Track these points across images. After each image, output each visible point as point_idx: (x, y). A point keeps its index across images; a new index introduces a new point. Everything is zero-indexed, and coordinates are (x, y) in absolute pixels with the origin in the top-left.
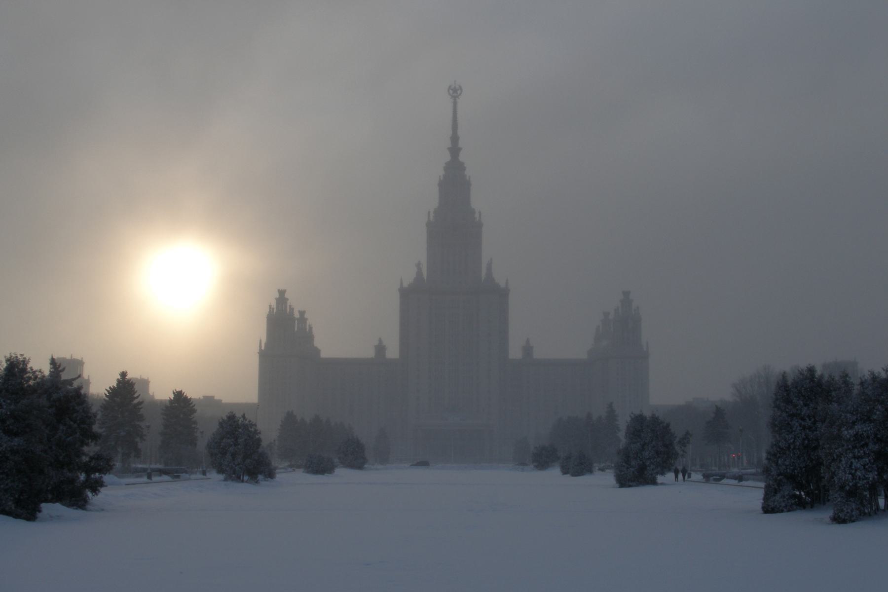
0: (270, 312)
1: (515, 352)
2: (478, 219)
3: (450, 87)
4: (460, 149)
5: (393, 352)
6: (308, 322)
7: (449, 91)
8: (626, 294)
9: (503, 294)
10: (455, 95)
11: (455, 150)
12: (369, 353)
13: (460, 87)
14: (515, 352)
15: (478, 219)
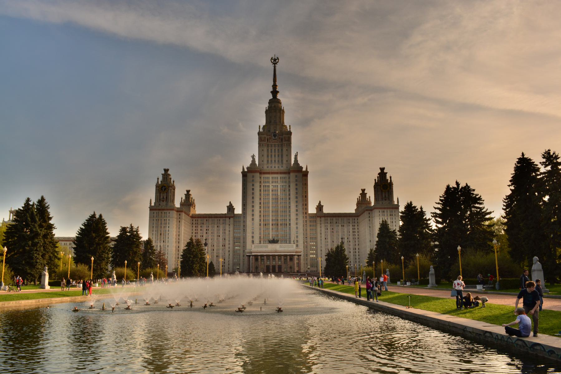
0: (158, 182)
1: (312, 210)
2: (289, 130)
3: (272, 58)
4: (278, 92)
5: (238, 210)
6: (191, 197)
7: (271, 60)
8: (382, 169)
9: (306, 174)
10: (275, 62)
11: (275, 92)
12: (225, 211)
13: (278, 58)
14: (312, 210)
15: (289, 130)
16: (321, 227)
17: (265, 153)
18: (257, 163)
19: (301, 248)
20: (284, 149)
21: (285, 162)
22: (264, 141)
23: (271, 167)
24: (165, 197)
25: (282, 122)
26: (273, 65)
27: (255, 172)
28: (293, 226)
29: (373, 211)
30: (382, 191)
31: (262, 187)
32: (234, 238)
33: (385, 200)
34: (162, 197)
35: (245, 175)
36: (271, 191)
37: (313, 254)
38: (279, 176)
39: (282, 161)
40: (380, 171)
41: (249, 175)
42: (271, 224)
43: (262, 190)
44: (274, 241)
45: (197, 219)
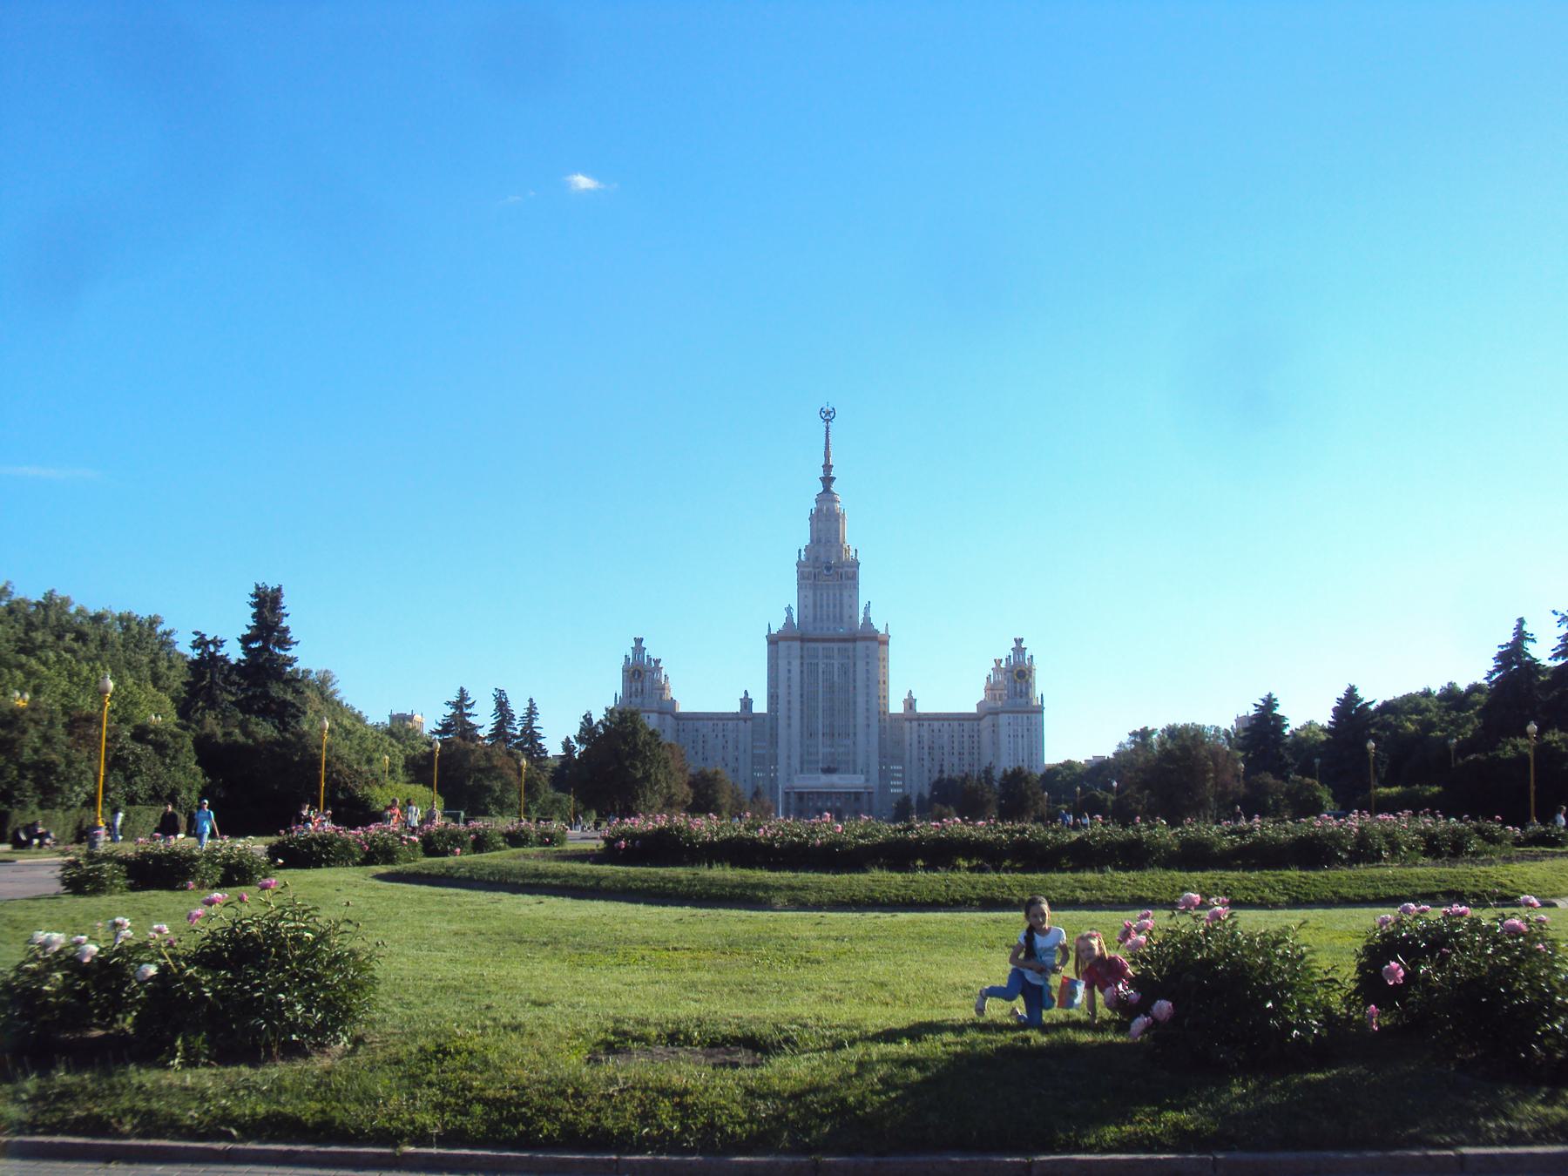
1: (896, 706)
5: (760, 706)
8: (1019, 641)
9: (884, 642)
11: (827, 480)
12: (736, 708)
14: (896, 706)
16: (911, 739)
17: (810, 601)
18: (796, 621)
19: (875, 776)
20: (846, 594)
21: (846, 619)
22: (808, 579)
23: (822, 629)
24: (640, 690)
25: (841, 540)
26: (825, 424)
27: (793, 639)
28: (861, 738)
29: (1001, 716)
30: (1015, 682)
31: (805, 666)
32: (754, 755)
33: (1021, 697)
34: (634, 689)
35: (773, 641)
36: (820, 671)
37: (896, 787)
38: (836, 646)
39: (841, 615)
40: (1014, 645)
41: (782, 644)
42: (821, 733)
43: (805, 671)
44: (828, 771)
45: (686, 722)
